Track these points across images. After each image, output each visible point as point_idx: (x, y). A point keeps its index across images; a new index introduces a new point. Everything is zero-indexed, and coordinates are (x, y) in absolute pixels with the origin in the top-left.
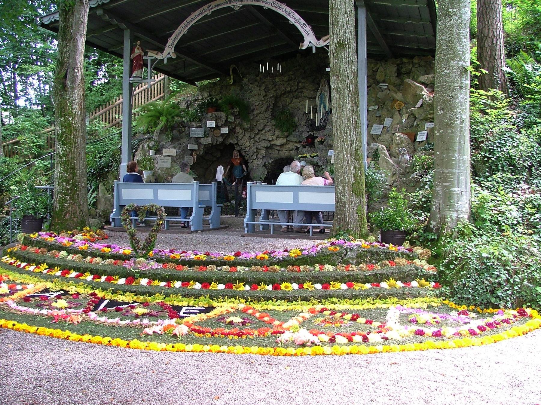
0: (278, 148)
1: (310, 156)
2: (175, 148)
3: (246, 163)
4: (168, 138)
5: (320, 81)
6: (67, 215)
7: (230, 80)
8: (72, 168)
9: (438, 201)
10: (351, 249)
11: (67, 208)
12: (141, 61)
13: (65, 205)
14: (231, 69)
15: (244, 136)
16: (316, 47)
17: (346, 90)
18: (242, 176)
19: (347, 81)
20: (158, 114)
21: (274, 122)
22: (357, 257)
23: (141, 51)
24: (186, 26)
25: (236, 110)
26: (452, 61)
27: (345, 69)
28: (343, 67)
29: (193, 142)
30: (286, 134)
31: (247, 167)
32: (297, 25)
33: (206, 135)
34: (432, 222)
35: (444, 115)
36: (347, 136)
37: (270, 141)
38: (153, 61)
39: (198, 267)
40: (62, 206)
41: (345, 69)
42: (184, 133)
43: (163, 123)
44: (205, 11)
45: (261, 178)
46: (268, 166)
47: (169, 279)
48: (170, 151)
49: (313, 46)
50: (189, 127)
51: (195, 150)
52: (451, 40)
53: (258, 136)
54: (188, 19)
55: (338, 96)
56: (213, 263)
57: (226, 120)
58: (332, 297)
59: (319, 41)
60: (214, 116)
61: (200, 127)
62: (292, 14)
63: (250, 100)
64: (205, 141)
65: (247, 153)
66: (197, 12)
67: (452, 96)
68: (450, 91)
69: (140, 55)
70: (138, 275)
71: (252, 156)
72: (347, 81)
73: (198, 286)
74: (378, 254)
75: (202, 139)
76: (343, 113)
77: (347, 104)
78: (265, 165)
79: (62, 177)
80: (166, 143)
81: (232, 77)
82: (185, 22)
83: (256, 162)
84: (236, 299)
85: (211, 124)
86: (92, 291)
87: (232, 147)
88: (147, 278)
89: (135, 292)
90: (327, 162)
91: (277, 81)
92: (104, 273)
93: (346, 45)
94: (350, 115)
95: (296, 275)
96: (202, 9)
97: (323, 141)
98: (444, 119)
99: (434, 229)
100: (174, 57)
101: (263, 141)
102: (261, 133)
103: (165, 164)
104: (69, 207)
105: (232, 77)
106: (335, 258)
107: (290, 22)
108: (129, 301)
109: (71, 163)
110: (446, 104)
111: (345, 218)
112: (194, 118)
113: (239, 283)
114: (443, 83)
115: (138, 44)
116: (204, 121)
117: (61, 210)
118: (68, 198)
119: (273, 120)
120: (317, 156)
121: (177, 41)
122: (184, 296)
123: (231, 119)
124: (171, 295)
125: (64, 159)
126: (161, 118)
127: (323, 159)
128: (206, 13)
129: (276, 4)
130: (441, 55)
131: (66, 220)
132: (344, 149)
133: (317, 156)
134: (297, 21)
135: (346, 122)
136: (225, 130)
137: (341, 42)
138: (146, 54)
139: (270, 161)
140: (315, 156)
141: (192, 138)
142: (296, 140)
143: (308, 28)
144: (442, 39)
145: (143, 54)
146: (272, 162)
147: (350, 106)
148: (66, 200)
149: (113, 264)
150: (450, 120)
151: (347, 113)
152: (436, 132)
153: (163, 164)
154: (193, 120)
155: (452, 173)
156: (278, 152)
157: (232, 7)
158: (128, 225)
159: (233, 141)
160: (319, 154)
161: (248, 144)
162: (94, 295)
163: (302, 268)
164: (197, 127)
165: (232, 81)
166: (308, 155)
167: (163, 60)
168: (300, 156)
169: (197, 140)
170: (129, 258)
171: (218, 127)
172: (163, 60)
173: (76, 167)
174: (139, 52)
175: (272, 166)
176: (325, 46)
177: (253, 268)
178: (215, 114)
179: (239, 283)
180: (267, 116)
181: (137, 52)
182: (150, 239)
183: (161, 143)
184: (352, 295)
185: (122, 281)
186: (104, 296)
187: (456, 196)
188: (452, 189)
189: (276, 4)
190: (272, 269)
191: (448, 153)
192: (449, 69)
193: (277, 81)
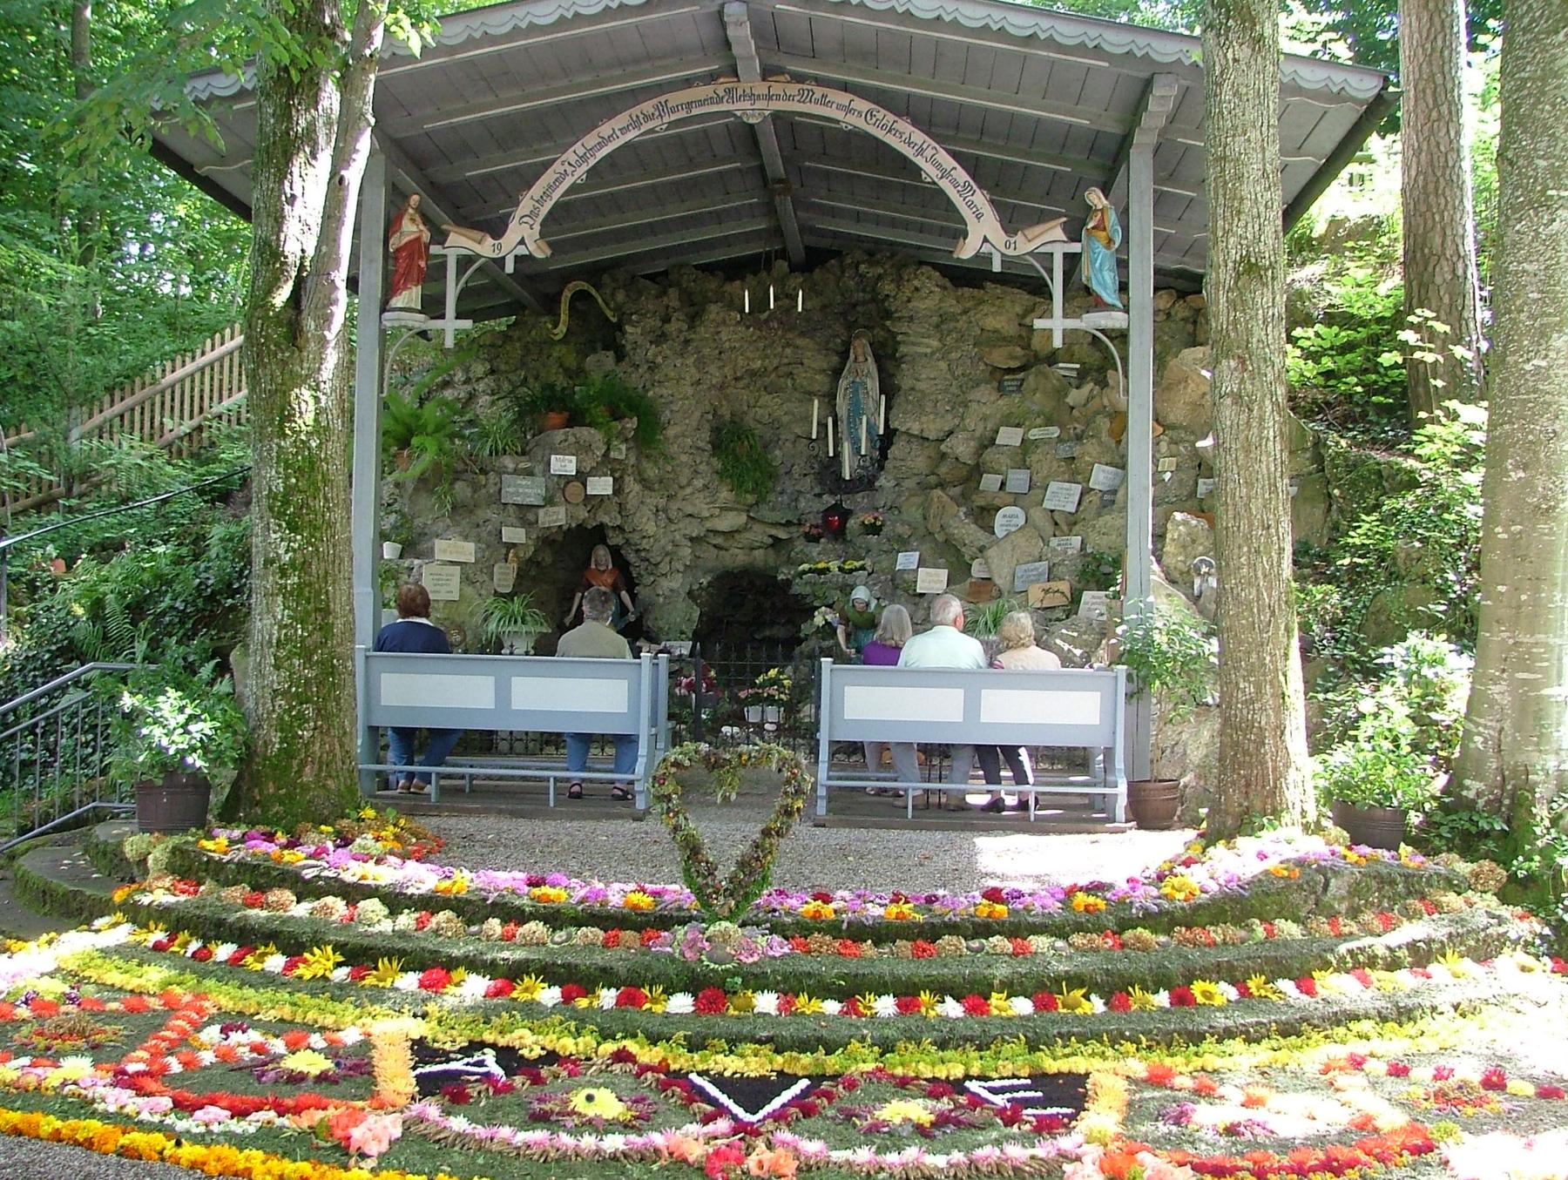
0: (719, 540)
1: (840, 569)
2: (466, 538)
3: (631, 585)
4: (443, 506)
5: (847, 346)
6: (307, 769)
7: (556, 326)
8: (320, 610)
9: (1494, 724)
10: (1335, 872)
11: (306, 745)
12: (420, 257)
13: (301, 737)
14: (567, 294)
16: (1003, 255)
17: (1267, 402)
19: (1270, 377)
20: (400, 429)
21: (717, 463)
22: (1349, 892)
23: (422, 227)
24: (583, 159)
25: (631, 424)
26: (1555, 335)
27: (1264, 338)
28: (1258, 333)
29: (515, 521)
30: (750, 499)
31: (633, 597)
32: (944, 184)
33: (549, 501)
34: (1467, 782)
35: (1527, 484)
36: (1269, 536)
37: (703, 519)
38: (465, 262)
39: (909, 944)
40: (289, 736)
41: (1264, 338)
42: (483, 491)
43: (428, 458)
44: (648, 118)
45: (682, 633)
46: (700, 595)
47: (850, 991)
48: (456, 549)
49: (993, 250)
50: (500, 474)
51: (514, 545)
52: (1552, 276)
53: (674, 506)
54: (591, 140)
55: (1244, 417)
56: (953, 928)
57: (606, 455)
58: (1356, 1018)
59: (1012, 240)
60: (572, 439)
61: (529, 473)
62: (929, 153)
63: (650, 394)
65: (643, 554)
66: (622, 120)
67: (1554, 432)
68: (1549, 419)
69: (418, 239)
70: (739, 980)
71: (656, 565)
72: (1270, 377)
73: (952, 1008)
74: (1393, 883)
75: (541, 512)
76: (1256, 467)
77: (1271, 444)
78: (690, 594)
79: (288, 639)
80: (434, 520)
81: (564, 317)
82: (578, 147)
83: (666, 585)
84: (1102, 1042)
85: (564, 464)
86: (609, 1047)
87: (599, 534)
88: (770, 990)
89: (769, 1040)
90: (896, 587)
91: (724, 339)
92: (607, 977)
93: (1267, 270)
94: (1278, 474)
95: (1213, 957)
96: (636, 111)
97: (879, 523)
98: (1528, 495)
99: (1481, 802)
100: (539, 255)
101: (688, 520)
102: (681, 494)
103: (444, 589)
104: (313, 743)
105: (564, 317)
106: (1296, 898)
107: (924, 175)
108: (763, 1072)
109: (318, 593)
110: (1535, 452)
111: (1265, 776)
112: (507, 444)
113: (1068, 992)
114: (1527, 393)
115: (412, 203)
116: (539, 452)
117: (288, 754)
118: (309, 711)
119: (713, 455)
120: (863, 568)
121: (548, 205)
122: (942, 1045)
123: (620, 451)
124: (901, 1045)
125: (296, 579)
126: (415, 441)
127: (882, 578)
128: (650, 125)
129: (880, 116)
130: (1523, 316)
131: (305, 788)
132: (1260, 574)
133: (863, 568)
134: (945, 174)
135: (1267, 496)
136: (601, 486)
137: (1253, 260)
138: (440, 237)
139: (704, 581)
140: (857, 570)
141: (509, 507)
142: (778, 520)
143: (980, 198)
144: (1524, 271)
145: (426, 236)
147: (1278, 447)
148: (302, 719)
149: (606, 945)
150: (1545, 497)
151: (1268, 469)
152: (1499, 529)
153: (438, 588)
154: (505, 451)
155: (1546, 645)
156: (716, 551)
157: (738, 113)
158: (676, 814)
159: (608, 518)
160: (868, 562)
161: (651, 528)
162: (622, 1056)
163: (1216, 934)
164: (516, 472)
165: (562, 329)
166: (834, 566)
167: (504, 258)
168: (805, 566)
169: (524, 513)
170: (664, 921)
171: (581, 477)
172: (504, 258)
173: (332, 605)
174: (414, 228)
175: (711, 595)
176: (1031, 253)
177: (1077, 939)
178: (574, 435)
179: (1068, 992)
180: (701, 444)
181: (411, 228)
182: (757, 859)
183: (417, 522)
184: (1399, 1008)
185: (682, 1003)
186: (664, 1059)
187: (1555, 710)
188: (1545, 692)
189: (880, 116)
190: (1138, 939)
191: (1538, 590)
192: (1546, 356)
193: (724, 339)
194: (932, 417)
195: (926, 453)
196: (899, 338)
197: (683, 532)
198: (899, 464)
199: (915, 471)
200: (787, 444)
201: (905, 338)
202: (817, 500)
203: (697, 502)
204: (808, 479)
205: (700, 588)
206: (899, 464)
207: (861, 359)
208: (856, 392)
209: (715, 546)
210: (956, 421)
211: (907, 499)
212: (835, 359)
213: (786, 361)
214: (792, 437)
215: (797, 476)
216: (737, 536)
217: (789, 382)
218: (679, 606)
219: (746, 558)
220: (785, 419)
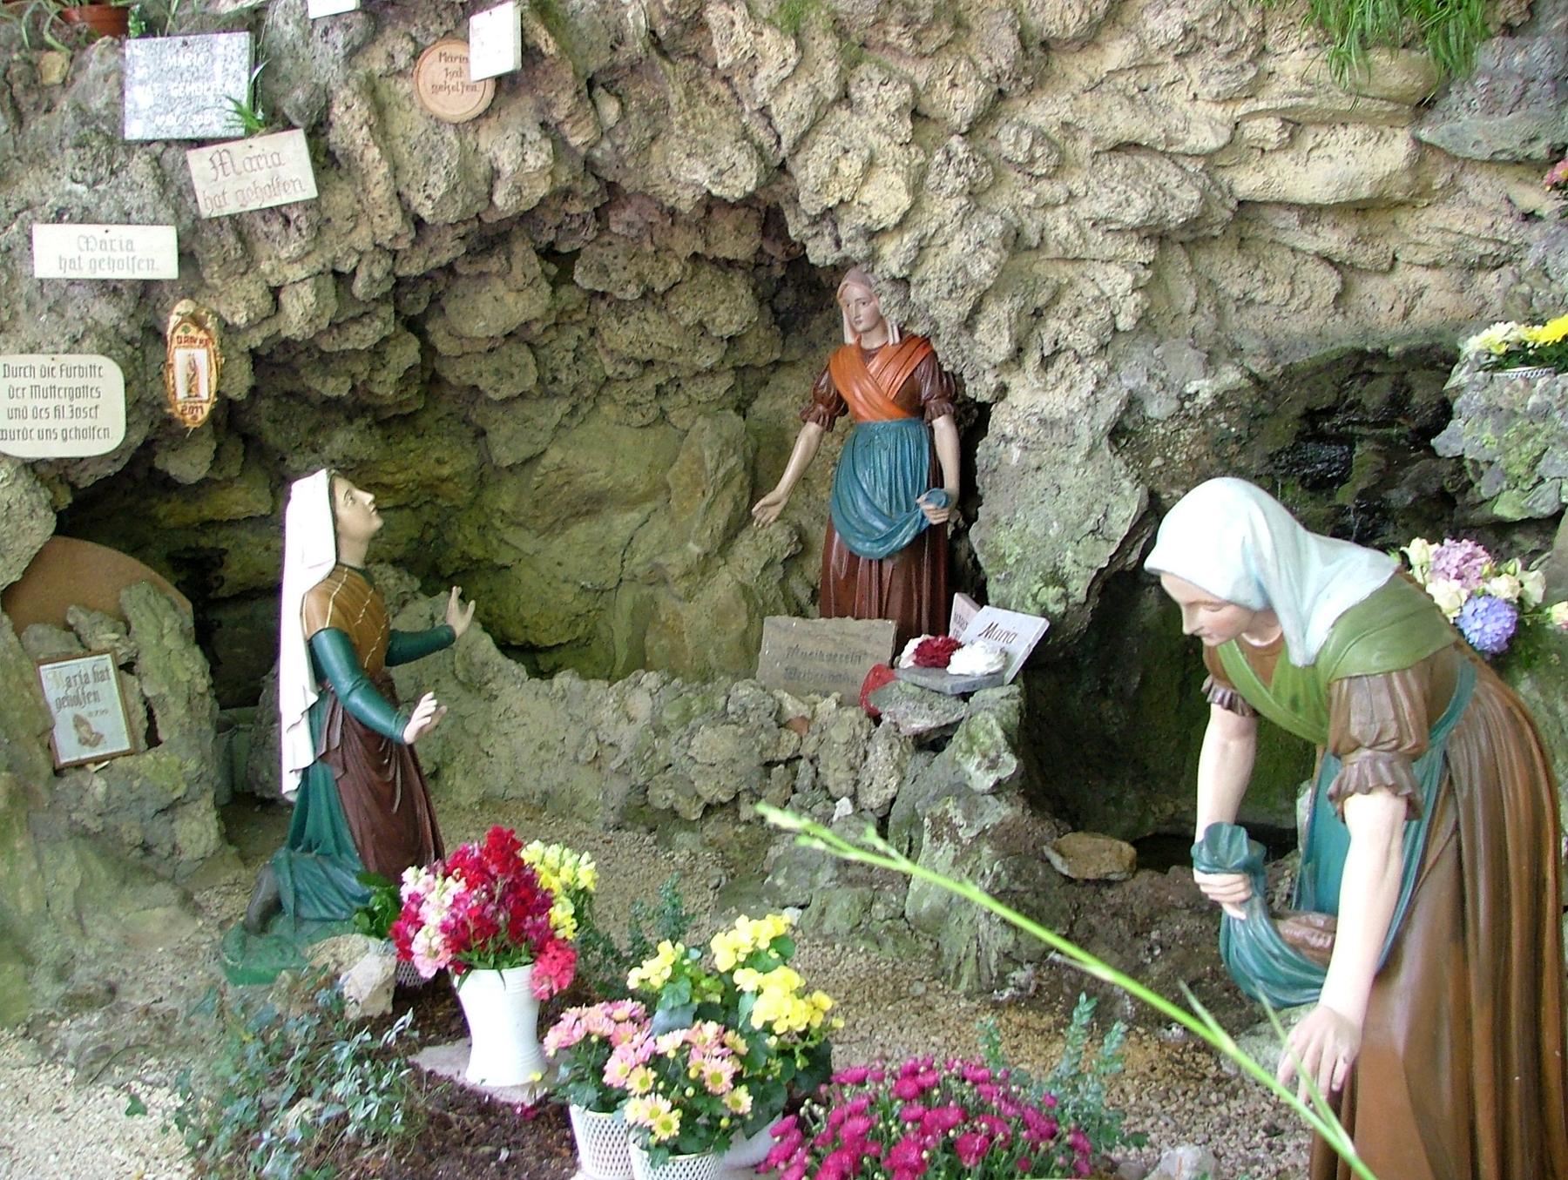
0: (1331, 239)
15: (845, 97)
18: (906, 536)
46: (1168, 441)
53: (1044, 112)
64: (230, 185)
139: (1204, 388)
142: (1512, 144)
146: (1219, 400)
197: (1084, 209)
203: (1180, 96)
205: (1182, 415)
209: (1327, 259)
216: (1403, 217)
218: (1068, 478)
219: (1446, 300)
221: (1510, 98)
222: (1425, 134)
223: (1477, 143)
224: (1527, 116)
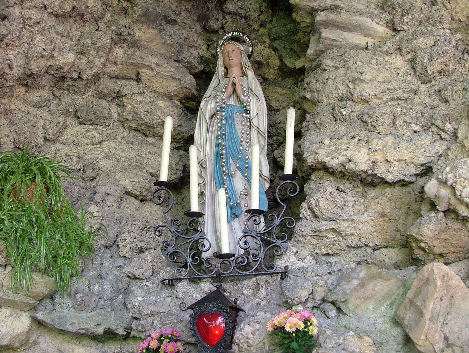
194: (390, 140)
195: (375, 207)
196: (321, 17)
198: (324, 225)
199: (354, 241)
200: (110, 200)
201: (331, 16)
202: (166, 291)
204: (148, 255)
206: (324, 225)
207: (235, 71)
208: (230, 118)
210: (440, 147)
211: (362, 284)
212: (189, 80)
213: (112, 69)
214: (118, 192)
215: (125, 251)
217: (114, 110)
220: (105, 164)
221: (92, 305)
222: (40, 316)
223: (73, 323)
224: (99, 314)
